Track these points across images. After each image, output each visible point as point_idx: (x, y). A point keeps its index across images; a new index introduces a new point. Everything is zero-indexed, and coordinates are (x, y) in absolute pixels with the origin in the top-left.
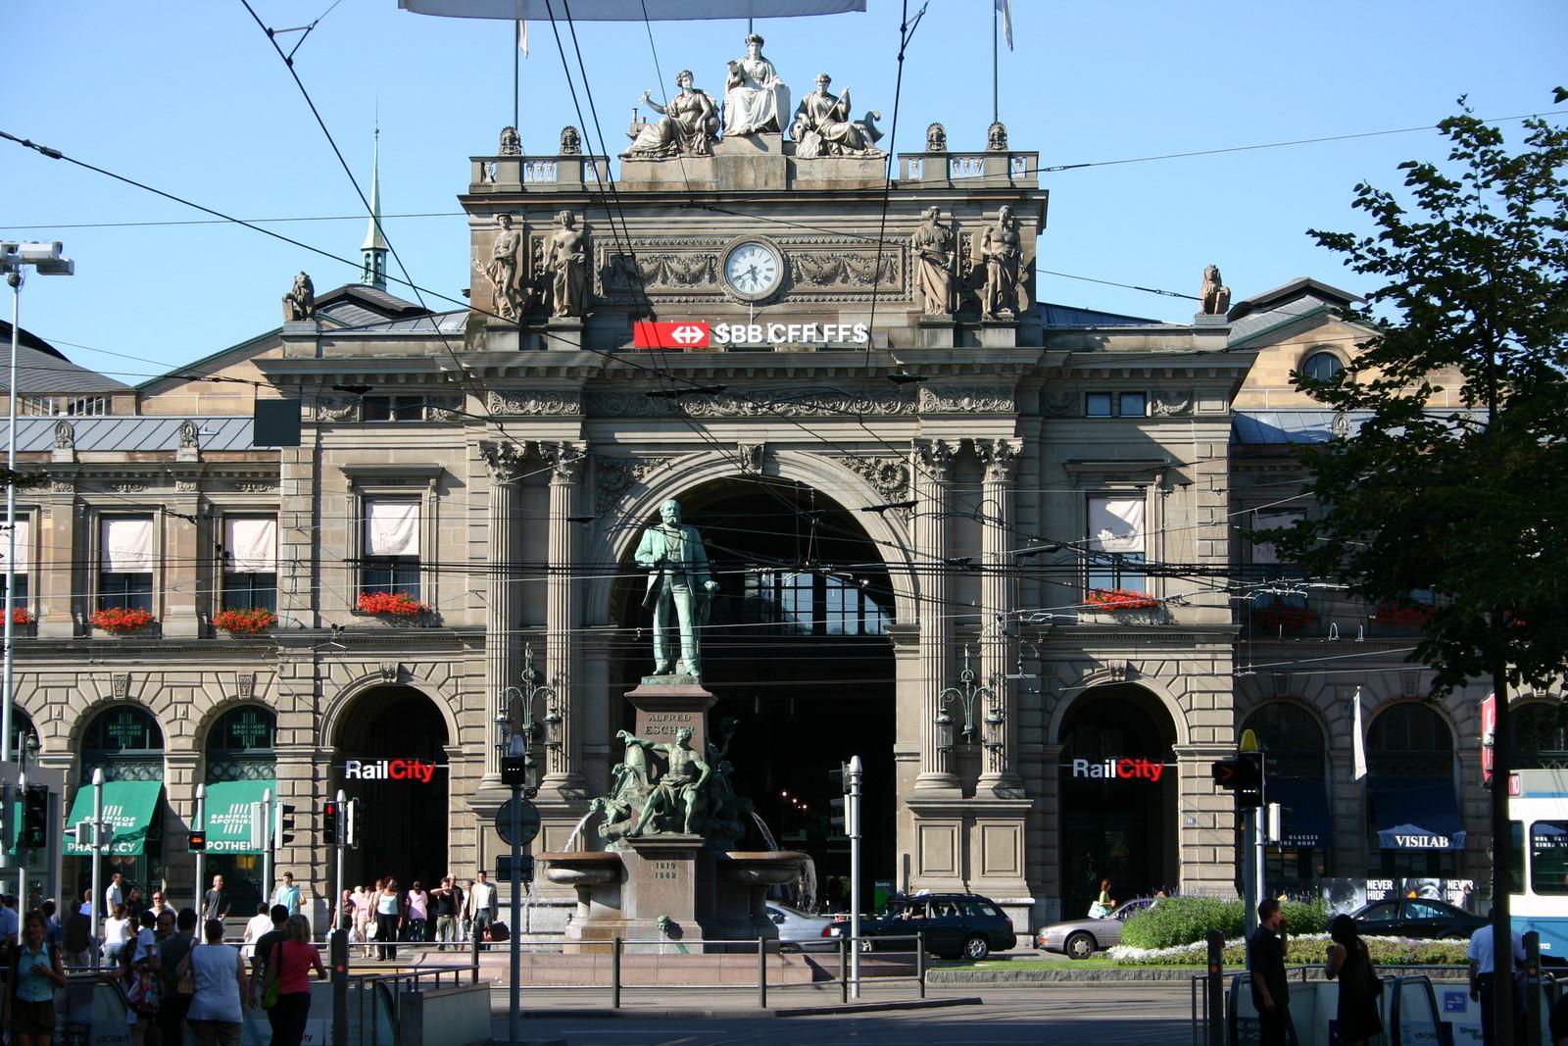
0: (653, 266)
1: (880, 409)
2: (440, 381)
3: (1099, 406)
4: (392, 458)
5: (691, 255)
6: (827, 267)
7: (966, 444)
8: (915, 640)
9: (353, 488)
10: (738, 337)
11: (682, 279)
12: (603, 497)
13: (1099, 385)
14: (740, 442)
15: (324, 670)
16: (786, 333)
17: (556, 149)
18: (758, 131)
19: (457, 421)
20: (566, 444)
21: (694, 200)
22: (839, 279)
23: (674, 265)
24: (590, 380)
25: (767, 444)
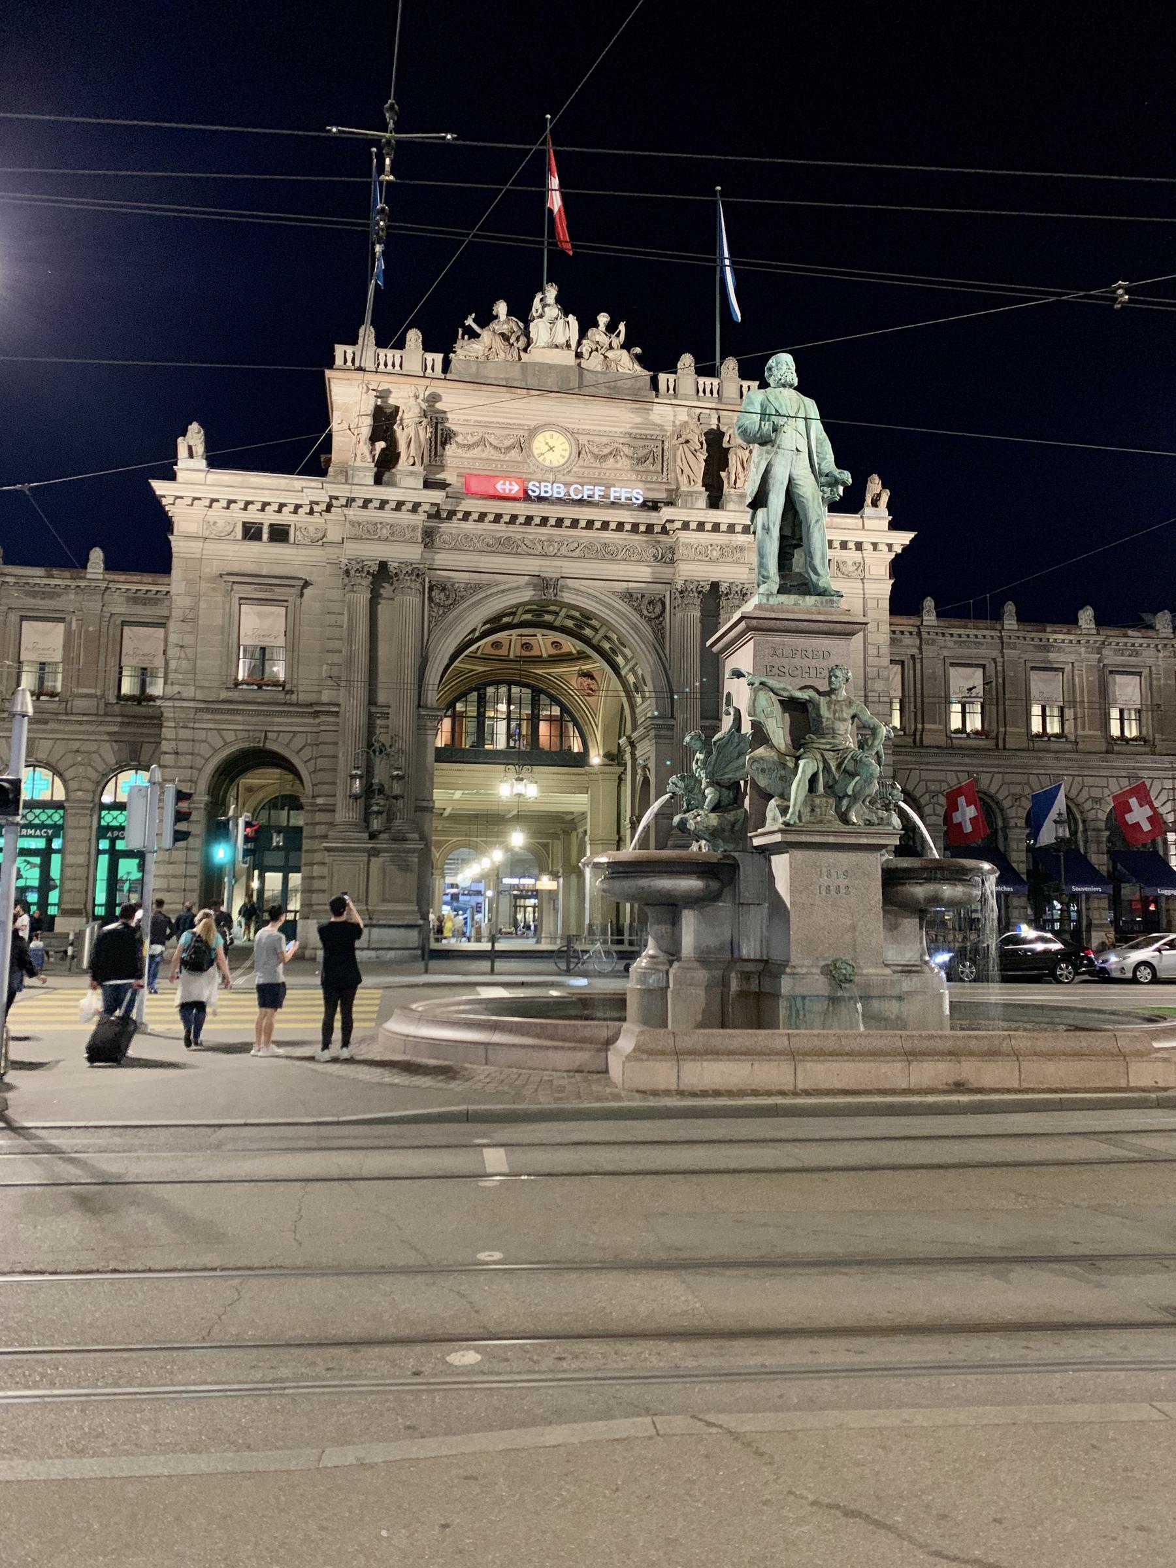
0: (475, 439)
5: (506, 432)
6: (606, 451)
7: (715, 585)
10: (546, 492)
15: (201, 735)
16: (582, 492)
23: (491, 440)
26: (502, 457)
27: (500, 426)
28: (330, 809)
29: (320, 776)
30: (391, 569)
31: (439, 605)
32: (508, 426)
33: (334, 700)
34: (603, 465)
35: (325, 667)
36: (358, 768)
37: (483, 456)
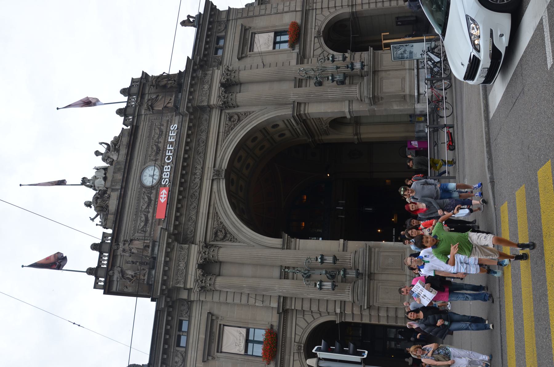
0: (143, 216)
1: (205, 123)
2: (171, 309)
3: (220, 52)
4: (202, 336)
6: (155, 148)
7: (222, 85)
8: (299, 104)
9: (213, 358)
11: (149, 205)
12: (227, 238)
13: (212, 50)
14: (211, 178)
16: (169, 156)
17: (97, 254)
18: (105, 174)
19: (189, 303)
20: (199, 252)
21: (122, 198)
22: (159, 145)
23: (144, 207)
24: (177, 240)
25: (214, 167)
26: (153, 202)
27: (139, 203)
28: (343, 303)
29: (323, 309)
30: (201, 262)
31: (225, 236)
32: (139, 200)
33: (277, 299)
34: (162, 149)
35: (257, 304)
36: (316, 284)
37: (151, 211)
